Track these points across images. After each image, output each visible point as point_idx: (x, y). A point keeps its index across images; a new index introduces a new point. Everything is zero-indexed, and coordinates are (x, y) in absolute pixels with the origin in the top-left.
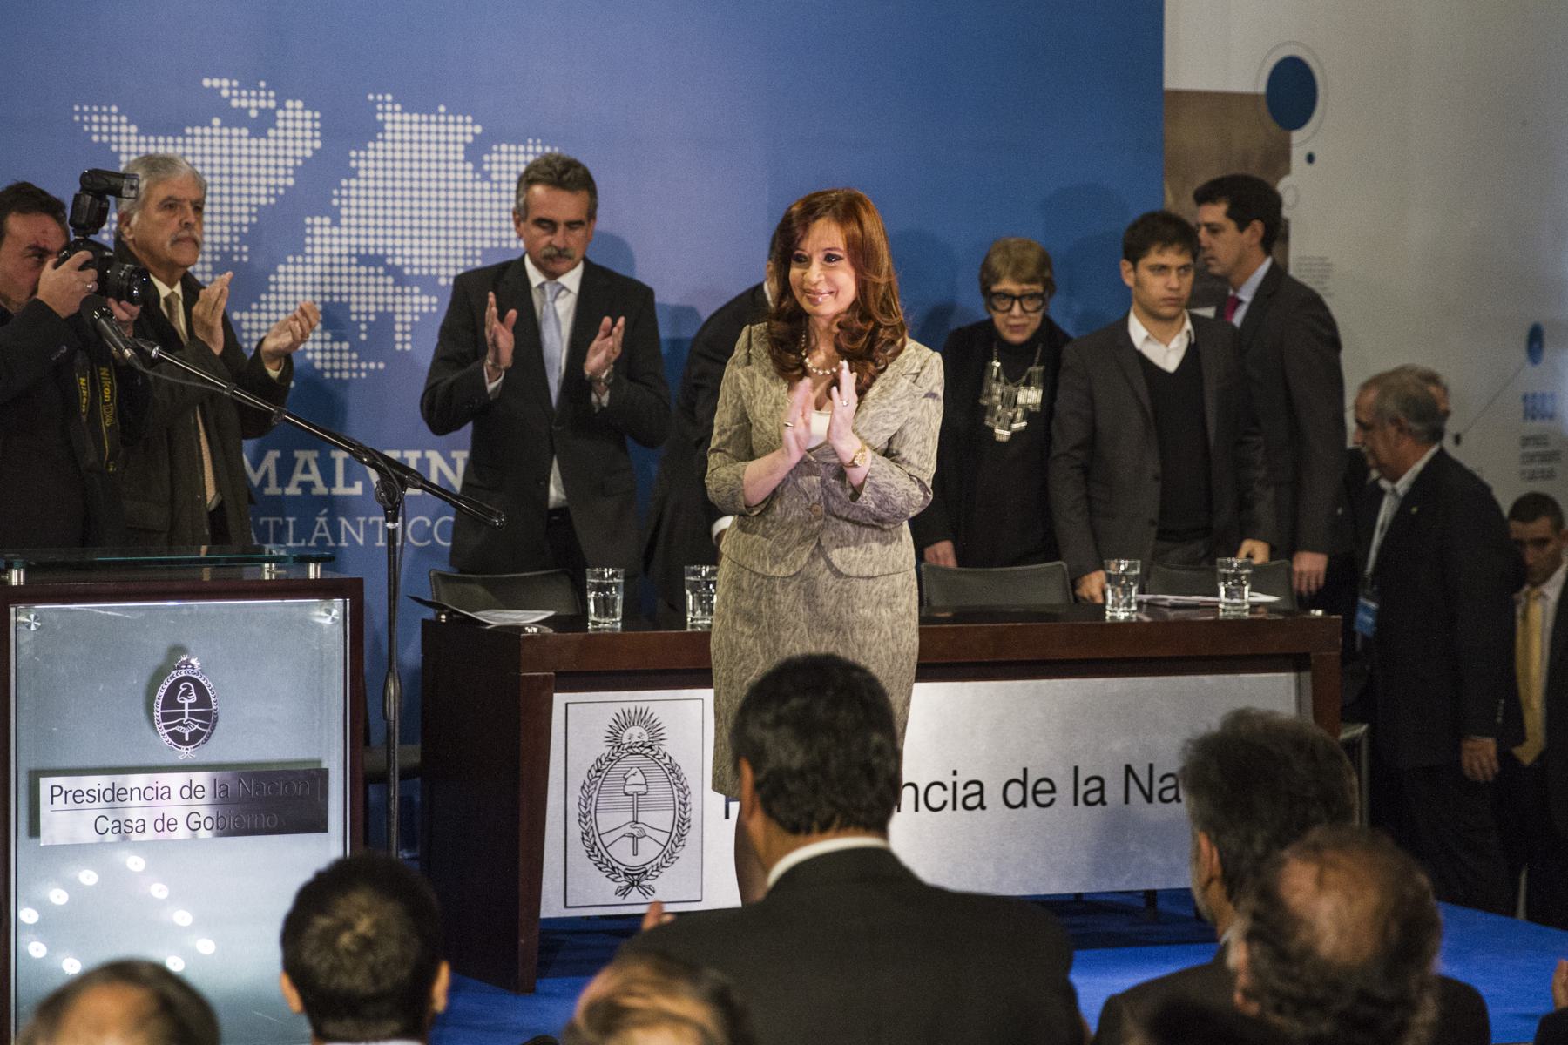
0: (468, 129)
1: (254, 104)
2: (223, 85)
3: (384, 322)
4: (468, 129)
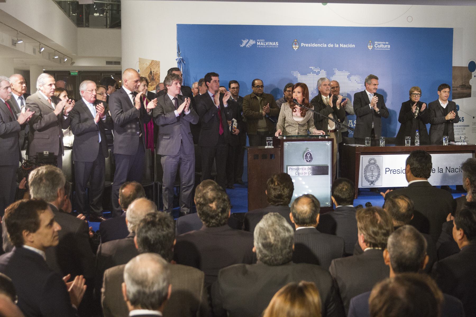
0: (348, 73)
1: (317, 70)
4: (348, 73)
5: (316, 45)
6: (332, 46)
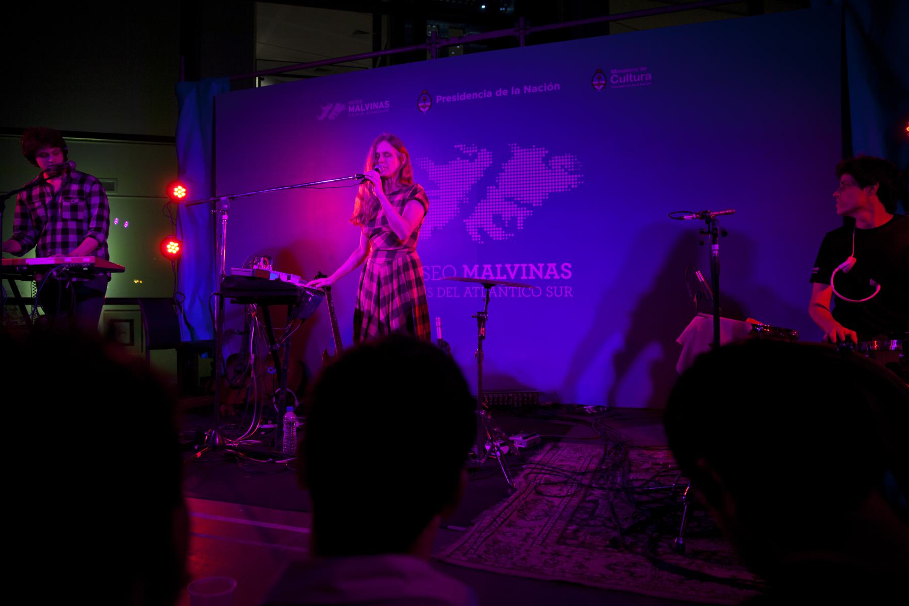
2: (460, 146)
3: (514, 220)
6: (505, 92)
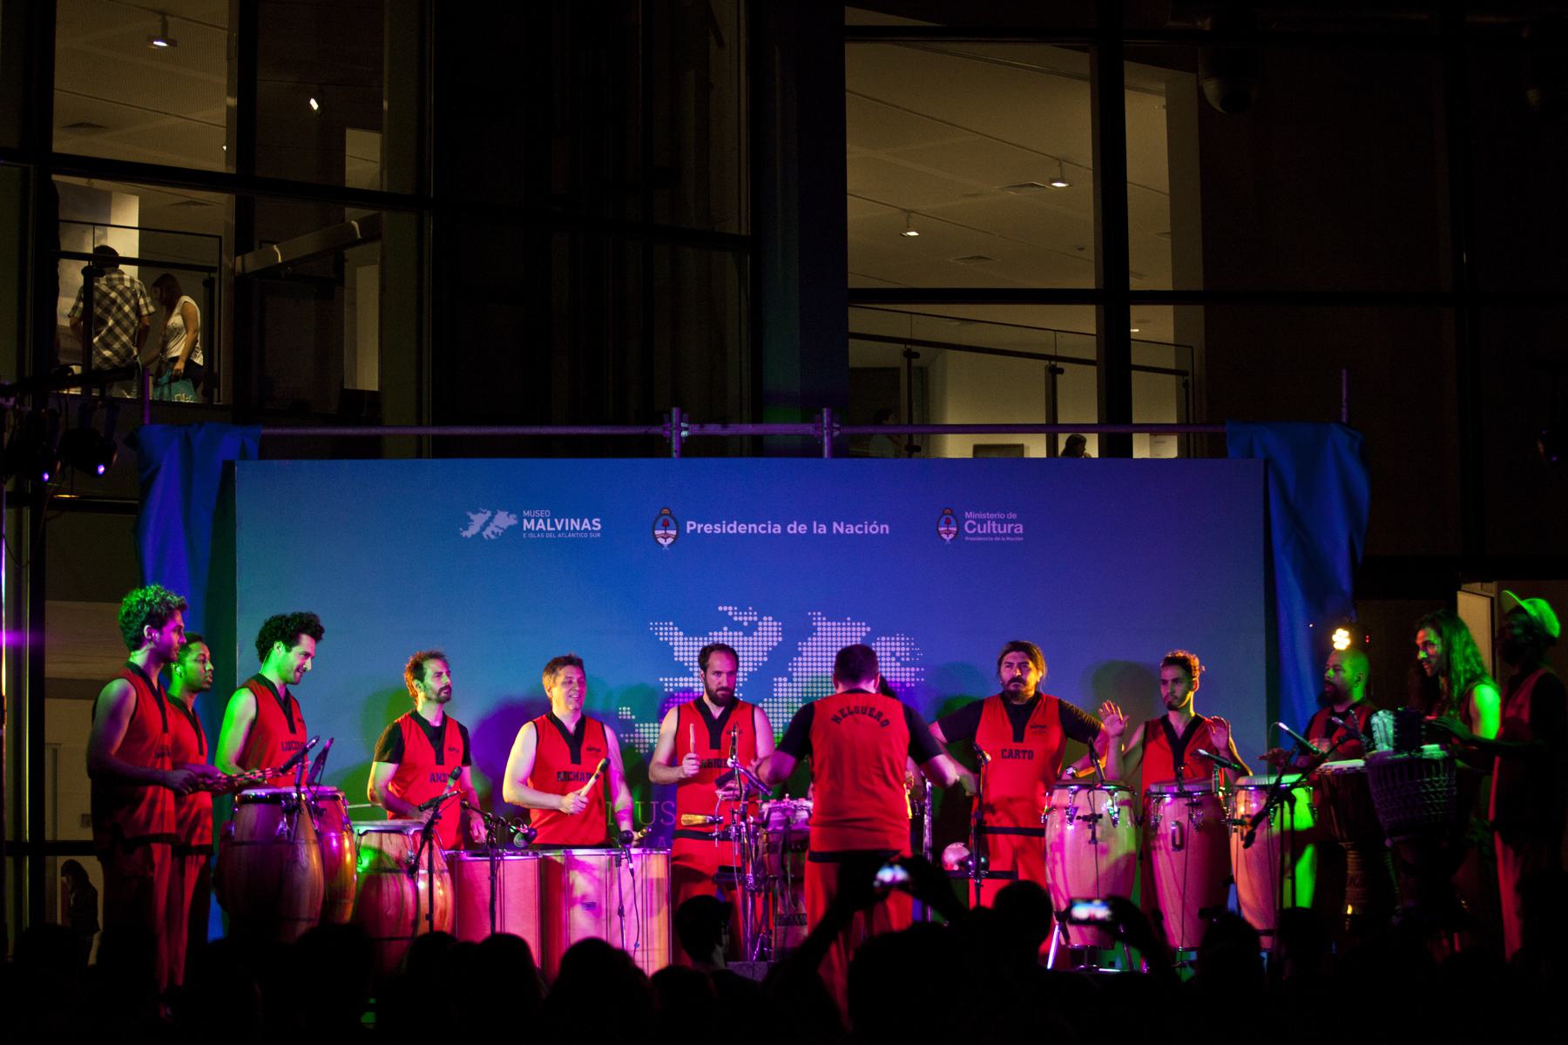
1: (745, 619)
5: (742, 528)
6: (803, 529)
